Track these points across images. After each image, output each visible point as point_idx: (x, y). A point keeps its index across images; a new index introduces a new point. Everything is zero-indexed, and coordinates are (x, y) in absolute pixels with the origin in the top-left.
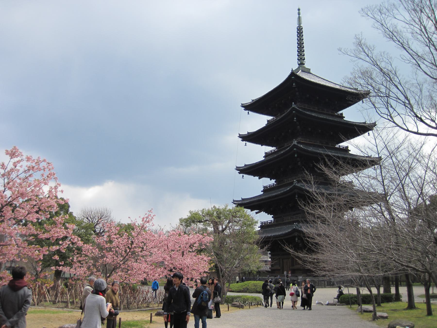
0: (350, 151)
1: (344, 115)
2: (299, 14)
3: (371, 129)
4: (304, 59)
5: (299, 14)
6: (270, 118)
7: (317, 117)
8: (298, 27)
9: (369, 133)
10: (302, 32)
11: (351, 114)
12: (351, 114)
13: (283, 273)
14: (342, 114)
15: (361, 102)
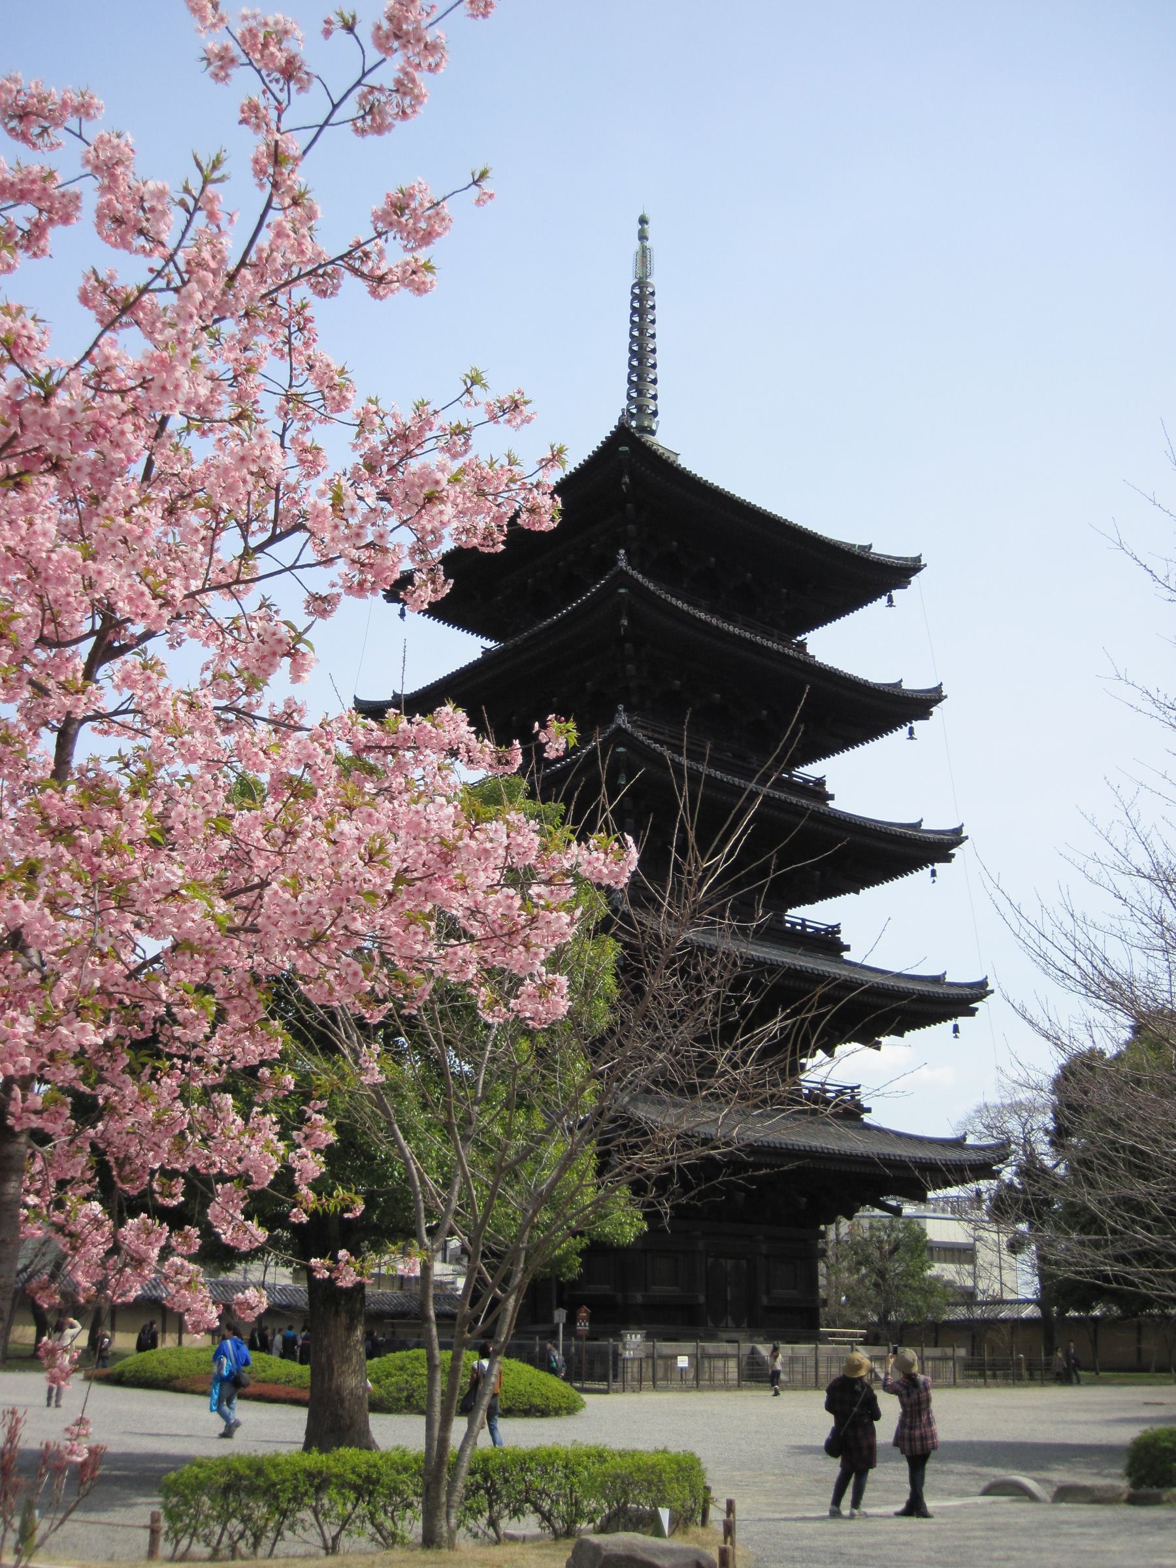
0: (832, 797)
1: (810, 650)
2: (643, 237)
3: (925, 714)
4: (655, 413)
5: (643, 237)
6: (490, 644)
7: (717, 627)
8: (633, 287)
9: (911, 731)
10: (653, 307)
11: (845, 645)
12: (845, 645)
13: (549, 1319)
14: (802, 645)
15: (885, 598)
